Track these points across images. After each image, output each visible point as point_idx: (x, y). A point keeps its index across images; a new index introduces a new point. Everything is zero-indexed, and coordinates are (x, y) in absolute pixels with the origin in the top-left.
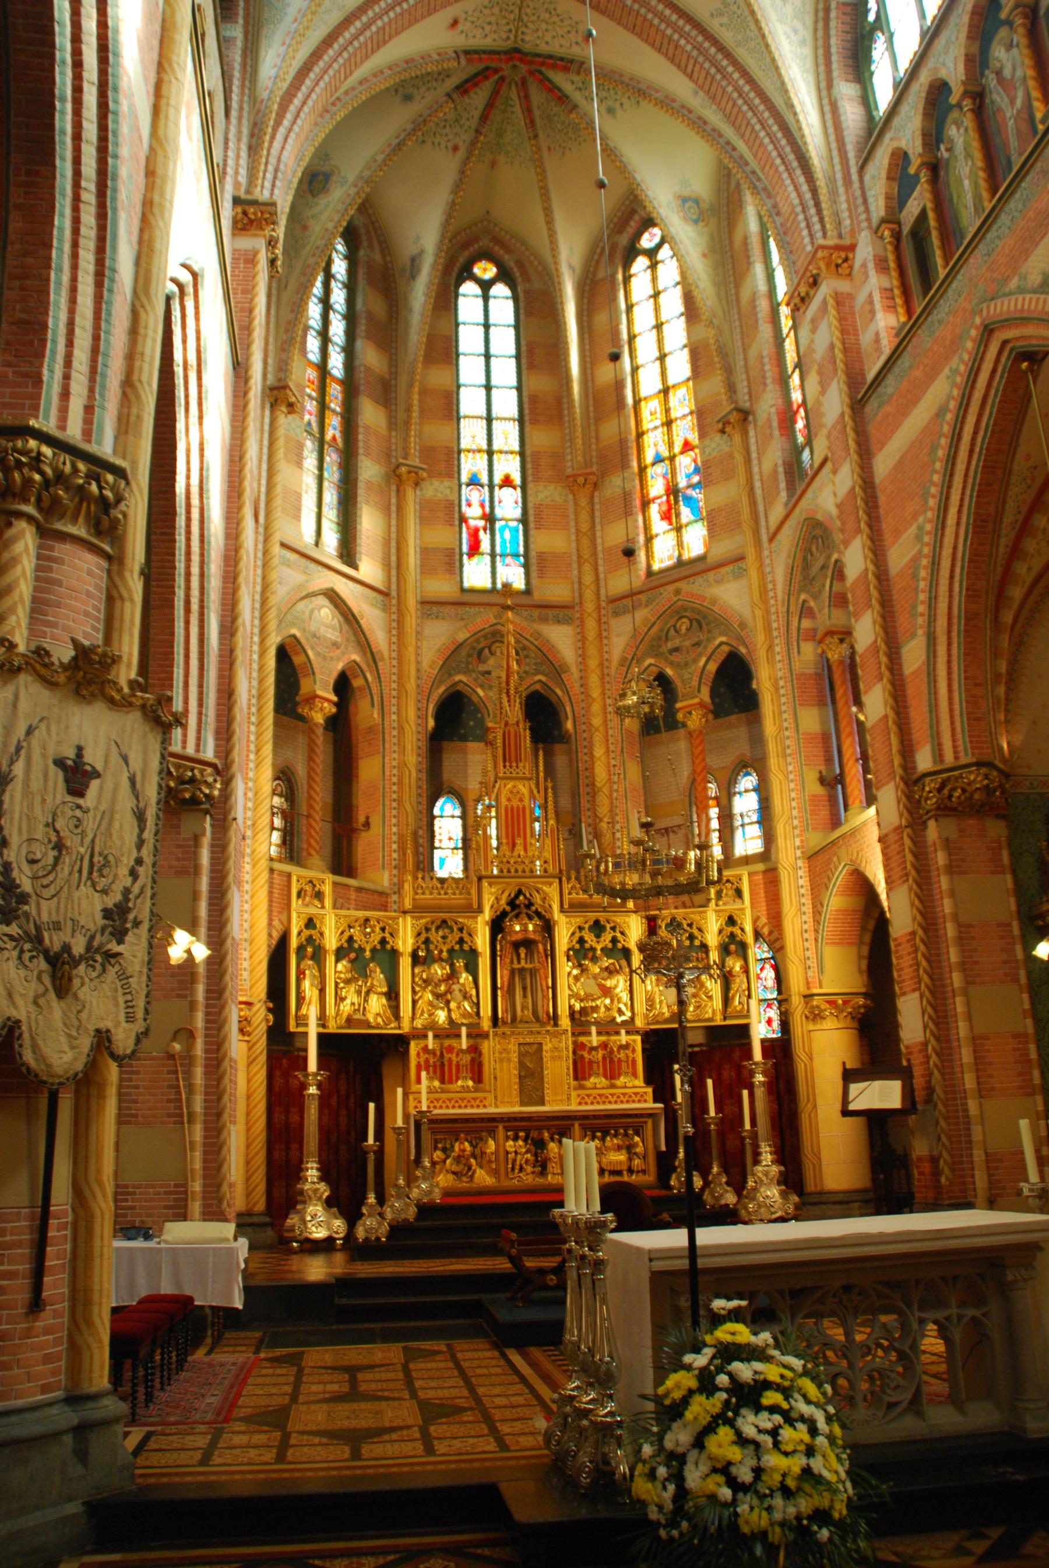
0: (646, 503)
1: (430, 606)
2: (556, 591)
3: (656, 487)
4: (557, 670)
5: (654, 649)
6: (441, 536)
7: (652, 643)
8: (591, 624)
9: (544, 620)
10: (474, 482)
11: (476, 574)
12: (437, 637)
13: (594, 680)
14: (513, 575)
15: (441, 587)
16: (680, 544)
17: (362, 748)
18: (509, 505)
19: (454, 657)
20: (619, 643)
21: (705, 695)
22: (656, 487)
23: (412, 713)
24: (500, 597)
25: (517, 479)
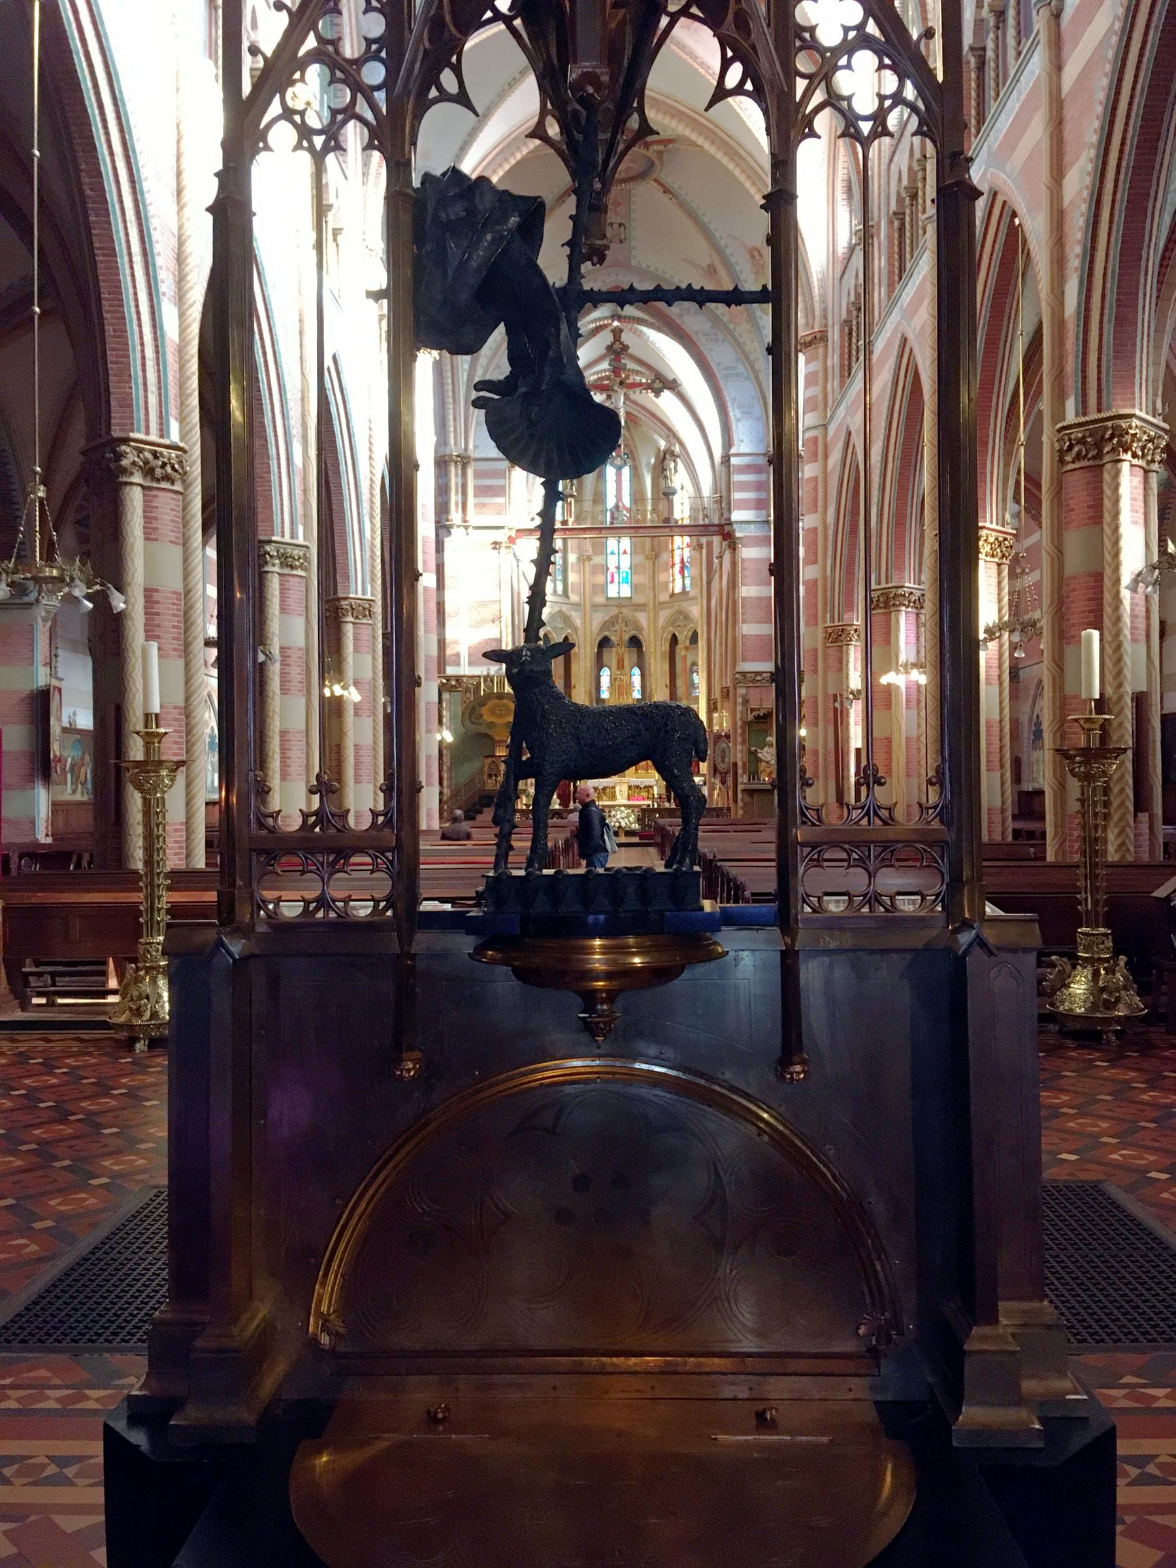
0: (673, 565)
1: (595, 607)
2: (640, 600)
3: (677, 560)
4: (640, 629)
5: (672, 624)
6: (600, 579)
7: (672, 622)
8: (652, 614)
9: (636, 611)
10: (612, 553)
11: (612, 592)
12: (599, 618)
13: (652, 635)
14: (626, 592)
15: (600, 599)
16: (684, 585)
17: (572, 660)
18: (626, 561)
19: (606, 625)
20: (661, 621)
21: (687, 643)
22: (677, 560)
23: (588, 649)
24: (620, 602)
25: (628, 551)
